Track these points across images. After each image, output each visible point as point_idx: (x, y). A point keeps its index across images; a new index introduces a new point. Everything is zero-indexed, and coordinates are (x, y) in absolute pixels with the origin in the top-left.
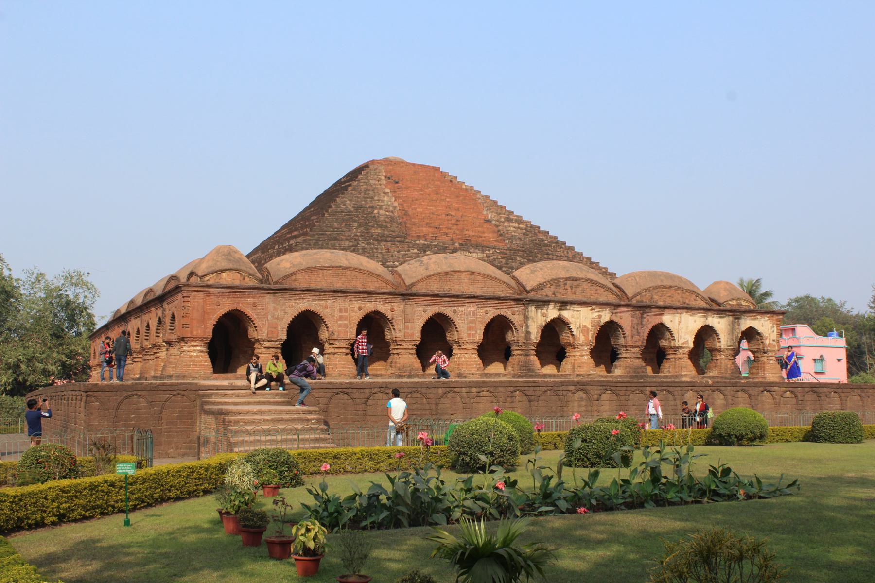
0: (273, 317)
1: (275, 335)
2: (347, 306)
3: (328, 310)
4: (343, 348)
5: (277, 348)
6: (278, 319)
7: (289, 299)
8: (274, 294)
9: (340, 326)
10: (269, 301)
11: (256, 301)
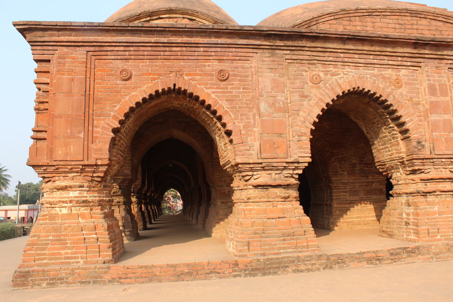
0: (272, 105)
1: (280, 153)
2: (444, 80)
3: (404, 90)
4: (443, 179)
5: (287, 186)
6: (285, 110)
7: (311, 62)
8: (273, 48)
9: (435, 127)
10: (261, 68)
11: (225, 66)
